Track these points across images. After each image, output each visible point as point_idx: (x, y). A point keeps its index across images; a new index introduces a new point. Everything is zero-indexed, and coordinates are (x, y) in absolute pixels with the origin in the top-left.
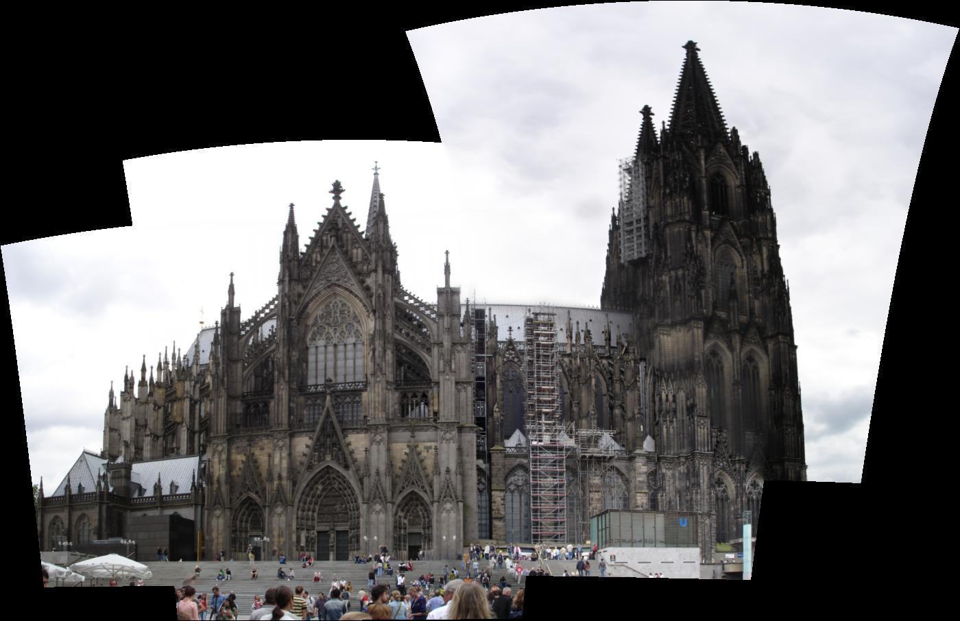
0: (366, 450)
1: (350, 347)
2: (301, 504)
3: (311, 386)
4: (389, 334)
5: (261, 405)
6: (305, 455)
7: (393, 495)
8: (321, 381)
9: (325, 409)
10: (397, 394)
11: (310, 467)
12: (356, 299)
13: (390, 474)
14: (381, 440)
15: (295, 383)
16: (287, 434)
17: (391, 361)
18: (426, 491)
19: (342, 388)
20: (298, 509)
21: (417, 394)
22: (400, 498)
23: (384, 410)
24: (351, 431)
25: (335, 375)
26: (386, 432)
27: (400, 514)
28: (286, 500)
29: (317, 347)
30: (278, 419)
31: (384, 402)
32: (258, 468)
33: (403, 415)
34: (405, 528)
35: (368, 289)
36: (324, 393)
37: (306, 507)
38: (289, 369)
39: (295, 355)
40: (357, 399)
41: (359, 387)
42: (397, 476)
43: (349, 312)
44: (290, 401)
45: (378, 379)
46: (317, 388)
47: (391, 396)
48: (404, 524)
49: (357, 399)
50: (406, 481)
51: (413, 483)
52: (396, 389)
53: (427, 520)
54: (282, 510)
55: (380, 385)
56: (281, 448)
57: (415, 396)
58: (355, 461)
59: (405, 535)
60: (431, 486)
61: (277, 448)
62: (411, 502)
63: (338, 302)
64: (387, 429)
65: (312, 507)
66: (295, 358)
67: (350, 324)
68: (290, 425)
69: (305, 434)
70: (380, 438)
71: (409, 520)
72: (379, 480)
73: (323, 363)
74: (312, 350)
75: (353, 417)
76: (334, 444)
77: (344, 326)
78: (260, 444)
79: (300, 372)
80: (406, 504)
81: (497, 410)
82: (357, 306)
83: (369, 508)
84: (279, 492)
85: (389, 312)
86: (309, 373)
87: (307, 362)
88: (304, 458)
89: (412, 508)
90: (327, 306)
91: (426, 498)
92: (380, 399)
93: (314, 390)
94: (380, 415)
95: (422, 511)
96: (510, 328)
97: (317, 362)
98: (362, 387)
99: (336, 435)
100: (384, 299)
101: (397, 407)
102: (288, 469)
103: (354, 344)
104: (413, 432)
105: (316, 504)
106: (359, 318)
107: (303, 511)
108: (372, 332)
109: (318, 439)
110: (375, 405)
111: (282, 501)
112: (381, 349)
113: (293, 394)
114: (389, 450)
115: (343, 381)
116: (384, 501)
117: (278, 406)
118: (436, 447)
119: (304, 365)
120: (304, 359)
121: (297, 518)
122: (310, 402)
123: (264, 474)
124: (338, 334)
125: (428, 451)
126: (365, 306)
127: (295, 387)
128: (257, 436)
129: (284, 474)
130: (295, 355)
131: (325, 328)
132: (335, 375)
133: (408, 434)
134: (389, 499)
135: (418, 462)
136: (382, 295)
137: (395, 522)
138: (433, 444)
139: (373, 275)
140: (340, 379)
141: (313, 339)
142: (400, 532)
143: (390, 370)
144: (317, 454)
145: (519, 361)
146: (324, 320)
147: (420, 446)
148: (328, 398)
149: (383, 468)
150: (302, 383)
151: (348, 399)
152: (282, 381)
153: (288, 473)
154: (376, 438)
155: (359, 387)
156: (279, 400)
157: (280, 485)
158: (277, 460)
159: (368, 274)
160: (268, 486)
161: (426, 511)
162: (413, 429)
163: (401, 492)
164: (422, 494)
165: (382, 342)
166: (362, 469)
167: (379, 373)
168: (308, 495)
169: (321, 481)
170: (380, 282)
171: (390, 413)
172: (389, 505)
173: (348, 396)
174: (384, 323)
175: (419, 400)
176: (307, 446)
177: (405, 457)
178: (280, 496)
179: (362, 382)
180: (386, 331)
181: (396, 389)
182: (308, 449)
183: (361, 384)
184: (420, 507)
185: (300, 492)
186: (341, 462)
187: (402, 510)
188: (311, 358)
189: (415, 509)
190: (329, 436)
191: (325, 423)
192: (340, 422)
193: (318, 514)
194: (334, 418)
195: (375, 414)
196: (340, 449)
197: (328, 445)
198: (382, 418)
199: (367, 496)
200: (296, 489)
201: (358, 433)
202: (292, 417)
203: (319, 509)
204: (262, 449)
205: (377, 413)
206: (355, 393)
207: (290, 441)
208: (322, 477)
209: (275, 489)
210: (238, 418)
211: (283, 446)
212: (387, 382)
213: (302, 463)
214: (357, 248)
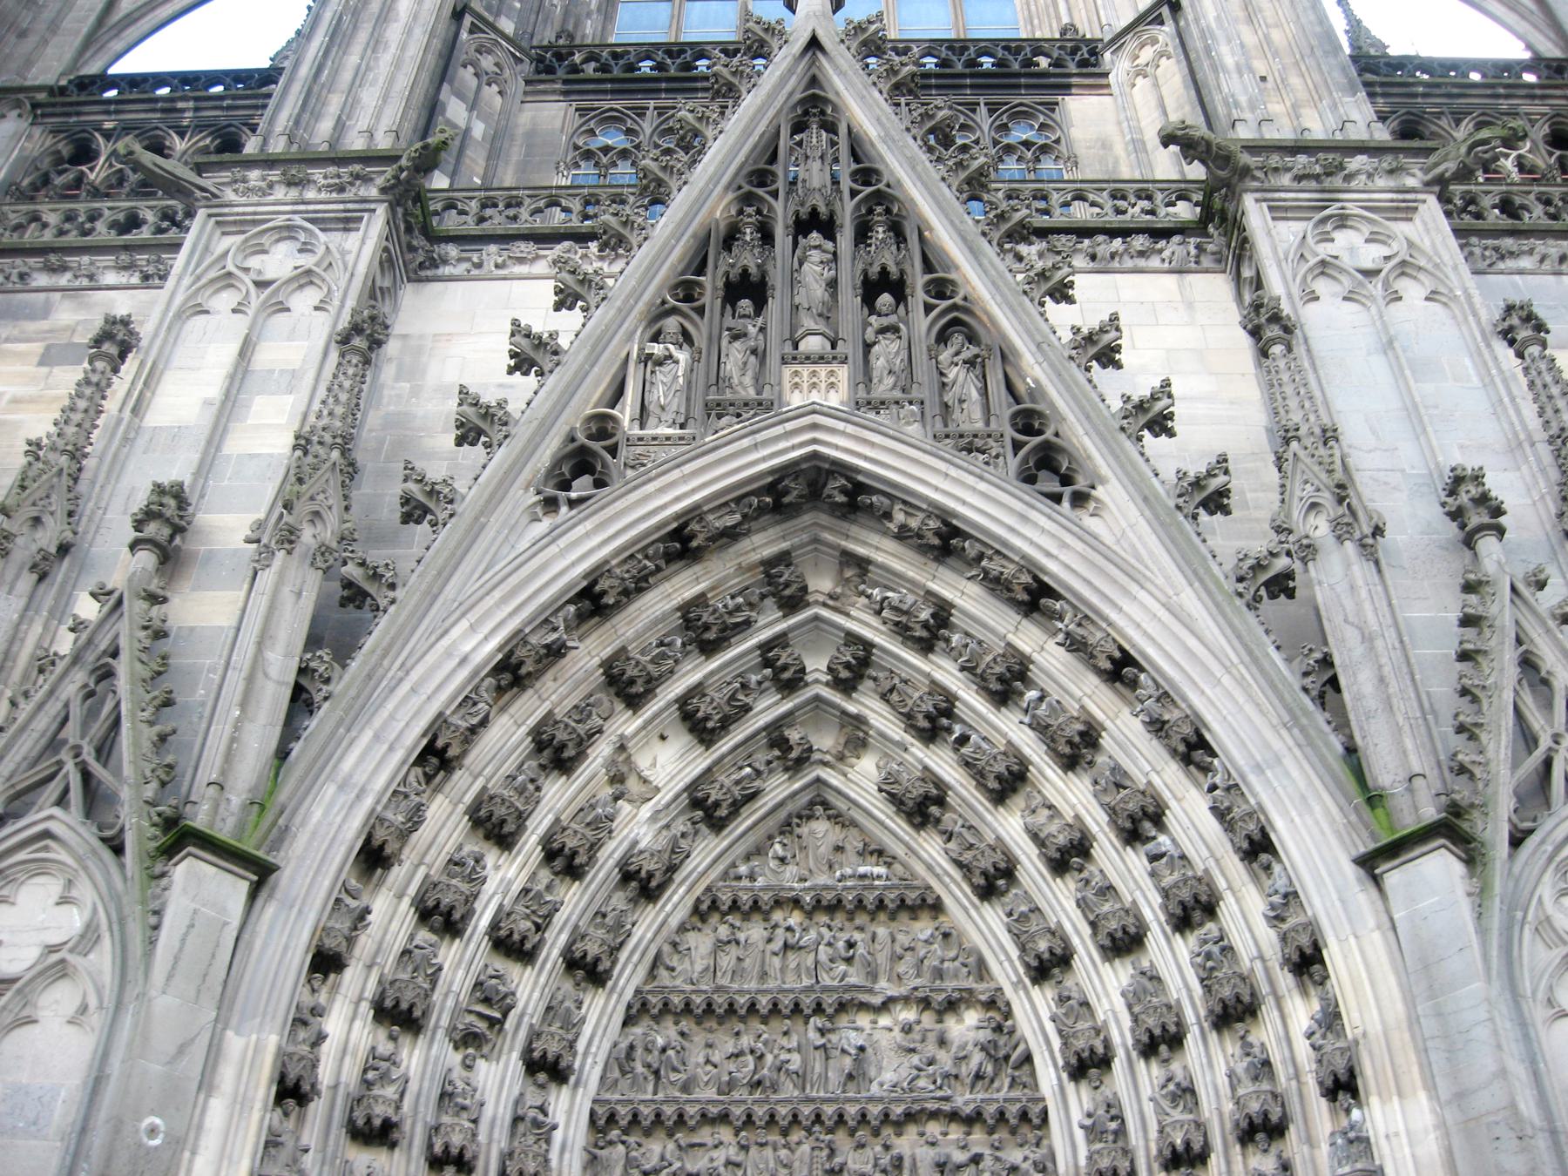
2: (390, 914)
11: (584, 464)
20: (326, 963)
37: (461, 963)
54: (73, 921)
61: (225, 301)
65: (530, 987)
105: (587, 970)
107: (398, 1016)
111: (94, 798)
121: (292, 1092)
168: (495, 827)
169: (693, 672)
178: (105, 749)
185: (403, 719)
193: (602, 1124)
197: (819, 292)
200: (346, 681)
203: (623, 1061)
208: (701, 631)
211: (305, 278)
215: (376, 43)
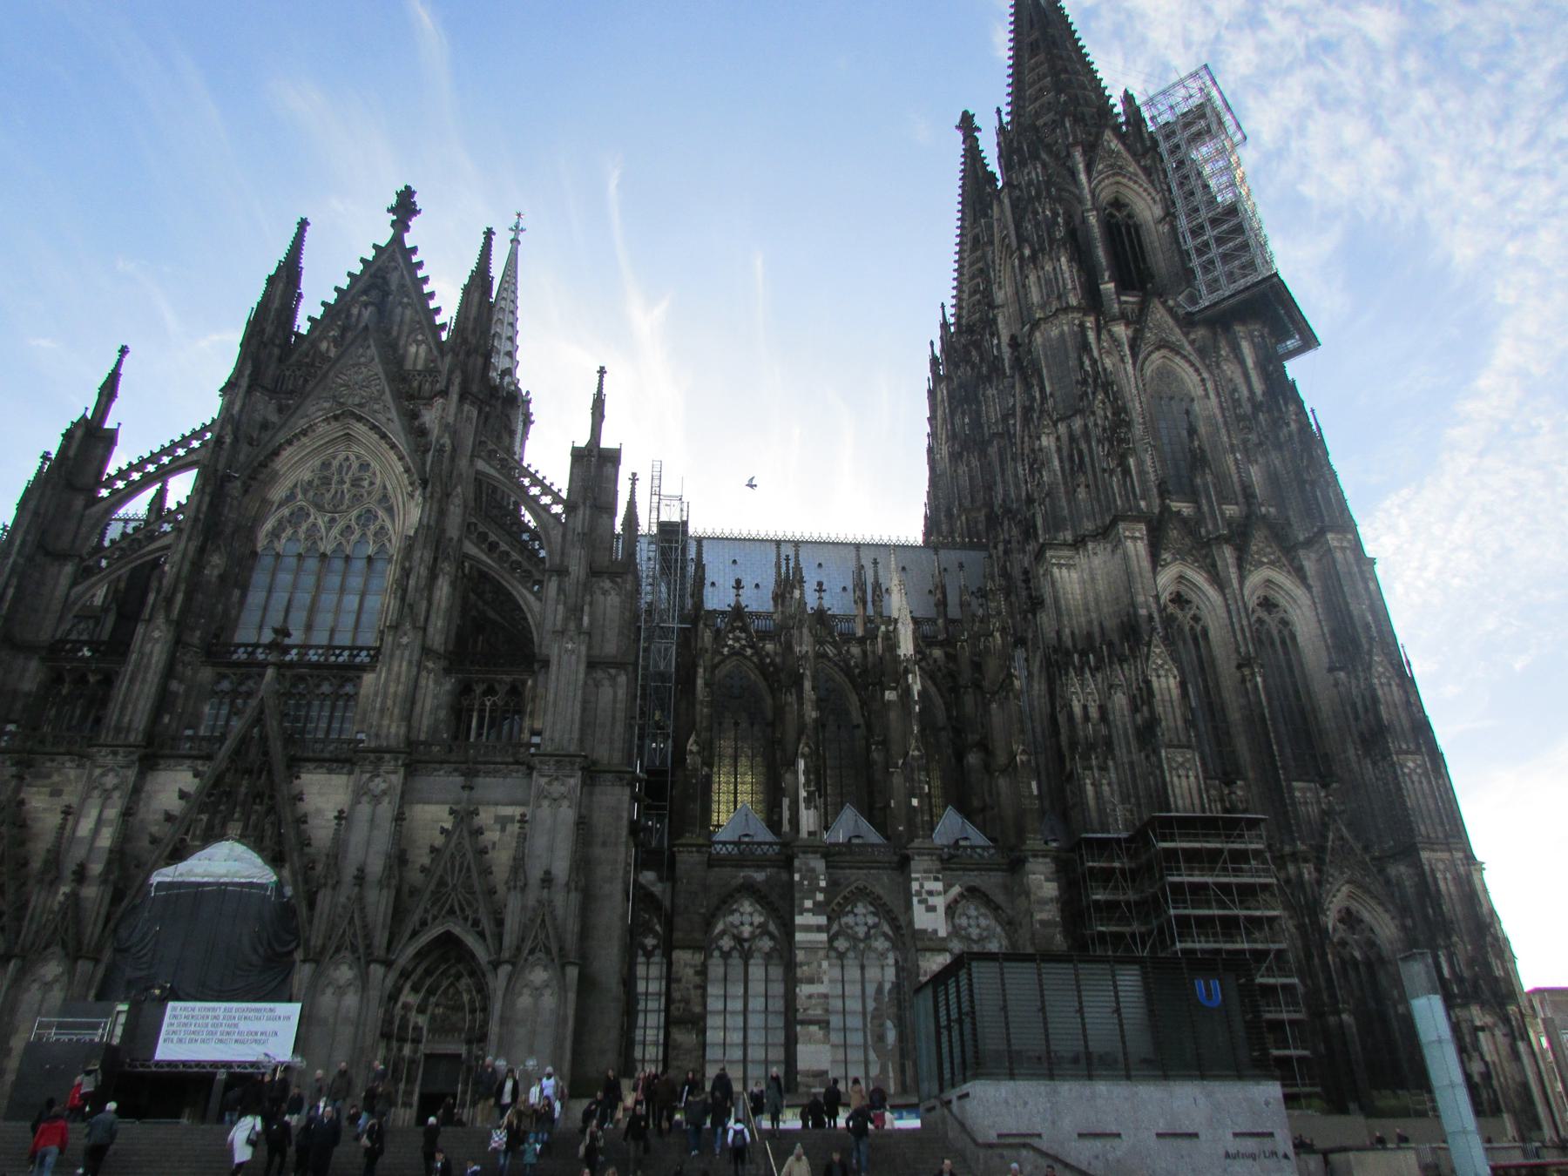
0: (340, 816)
1: (359, 565)
3: (239, 646)
4: (451, 539)
5: (92, 679)
6: (169, 817)
7: (390, 943)
8: (268, 636)
9: (253, 702)
10: (448, 684)
12: (392, 453)
13: (394, 882)
14: (384, 793)
15: (198, 633)
16: (135, 757)
17: (444, 605)
18: (482, 935)
19: (315, 658)
21: (497, 686)
22: (411, 951)
23: (408, 718)
24: (311, 766)
25: (309, 627)
26: (402, 771)
27: (408, 997)
28: (79, 943)
29: (278, 556)
30: (122, 714)
31: (411, 700)
32: (23, 843)
33: (455, 738)
34: (416, 1041)
35: (422, 432)
36: (264, 665)
38: (189, 597)
39: (217, 562)
40: (349, 689)
41: (358, 660)
42: (414, 892)
43: (372, 484)
44: (169, 672)
45: (405, 640)
46: (253, 653)
47: (431, 683)
48: (417, 1028)
49: (349, 689)
50: (434, 904)
51: (451, 912)
52: (447, 671)
53: (479, 1015)
55: (407, 653)
56: (107, 795)
57: (490, 691)
58: (305, 842)
59: (412, 1061)
60: (500, 923)
62: (443, 967)
63: (352, 458)
64: (406, 766)
66: (216, 572)
67: (369, 511)
68: (151, 737)
69: (188, 762)
70: (383, 786)
71: (433, 1018)
72: (360, 898)
73: (286, 596)
74: (267, 561)
75: (328, 732)
76: (258, 796)
77: (355, 513)
78: (56, 778)
79: (220, 607)
80: (428, 972)
81: (695, 748)
82: (390, 470)
83: (317, 976)
84: (63, 918)
85: (459, 489)
86: (245, 616)
87: (245, 589)
88: (167, 826)
89: (445, 984)
90: (326, 465)
91: (482, 954)
92: (401, 688)
93: (244, 656)
94: (393, 730)
95: (469, 992)
96: (738, 582)
97: (270, 591)
98: (367, 660)
99: (270, 772)
100: (453, 459)
101: (442, 714)
102: (111, 851)
103: (370, 559)
104: (470, 773)
106: (393, 500)
108: (412, 533)
109: (218, 781)
110: (384, 702)
112: (423, 571)
113: (187, 658)
114: (399, 818)
115: (325, 642)
116: (364, 959)
117: (132, 681)
118: (523, 815)
119: (237, 593)
120: (238, 578)
122: (225, 685)
123: (36, 865)
124: (335, 531)
125: (503, 829)
126: (407, 470)
127: (196, 641)
128: (52, 756)
129: (96, 868)
130: (217, 562)
131: (308, 515)
132: (309, 627)
133: (459, 780)
134: (380, 952)
135: (470, 855)
136: (448, 448)
137: (388, 1020)
138: (516, 811)
139: (439, 401)
140: (320, 638)
141: (275, 534)
142: (400, 1049)
143: (439, 624)
144: (204, 817)
145: (757, 652)
146: (311, 494)
147: (483, 815)
148: (270, 673)
149: (376, 867)
150: (217, 636)
151: (326, 688)
152: (160, 620)
153: (109, 863)
154: (372, 785)
155: (358, 660)
156: (138, 665)
157: (74, 898)
158: (85, 827)
159: (429, 401)
160: (37, 898)
161: (481, 989)
162: (470, 773)
163: (414, 934)
164: (470, 940)
165: (428, 556)
166: (320, 867)
167: (408, 626)
170: (451, 420)
171: (424, 728)
172: (377, 970)
173: (327, 679)
174: (442, 513)
175: (500, 703)
176: (183, 795)
177: (439, 841)
179: (368, 649)
180: (443, 531)
181: (447, 671)
182: (183, 803)
183: (364, 653)
184: (465, 981)
186: (267, 842)
187: (415, 989)
188: (260, 578)
189: (452, 984)
190: (249, 772)
191: (244, 740)
192: (289, 740)
194: (272, 725)
195: (380, 726)
196: (271, 810)
197: (241, 797)
198: (397, 734)
199: (320, 942)
201: (330, 772)
202: (166, 719)
204: (56, 793)
205: (386, 722)
206: (343, 671)
207: (142, 775)
209: (56, 907)
210: (19, 706)
211: (116, 788)
212: (426, 651)
213: (154, 841)
214: (418, 343)
215: (144, 680)
